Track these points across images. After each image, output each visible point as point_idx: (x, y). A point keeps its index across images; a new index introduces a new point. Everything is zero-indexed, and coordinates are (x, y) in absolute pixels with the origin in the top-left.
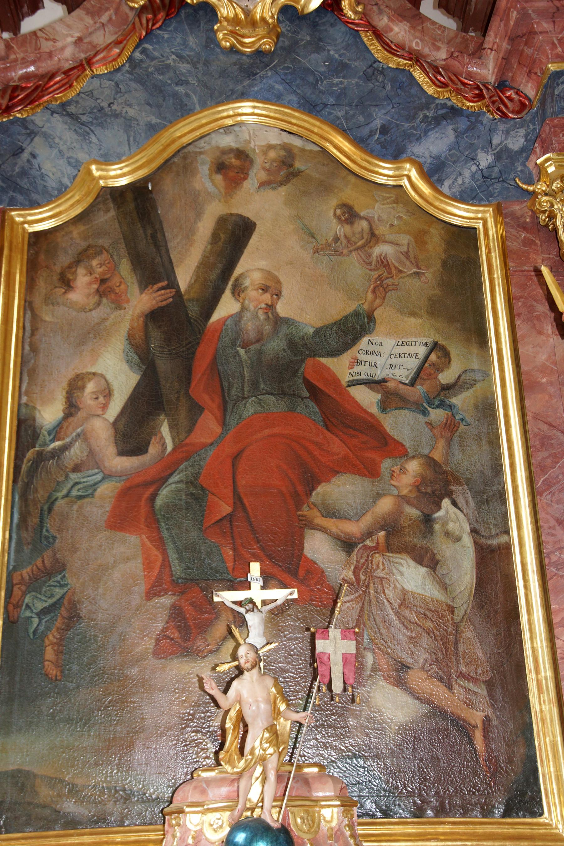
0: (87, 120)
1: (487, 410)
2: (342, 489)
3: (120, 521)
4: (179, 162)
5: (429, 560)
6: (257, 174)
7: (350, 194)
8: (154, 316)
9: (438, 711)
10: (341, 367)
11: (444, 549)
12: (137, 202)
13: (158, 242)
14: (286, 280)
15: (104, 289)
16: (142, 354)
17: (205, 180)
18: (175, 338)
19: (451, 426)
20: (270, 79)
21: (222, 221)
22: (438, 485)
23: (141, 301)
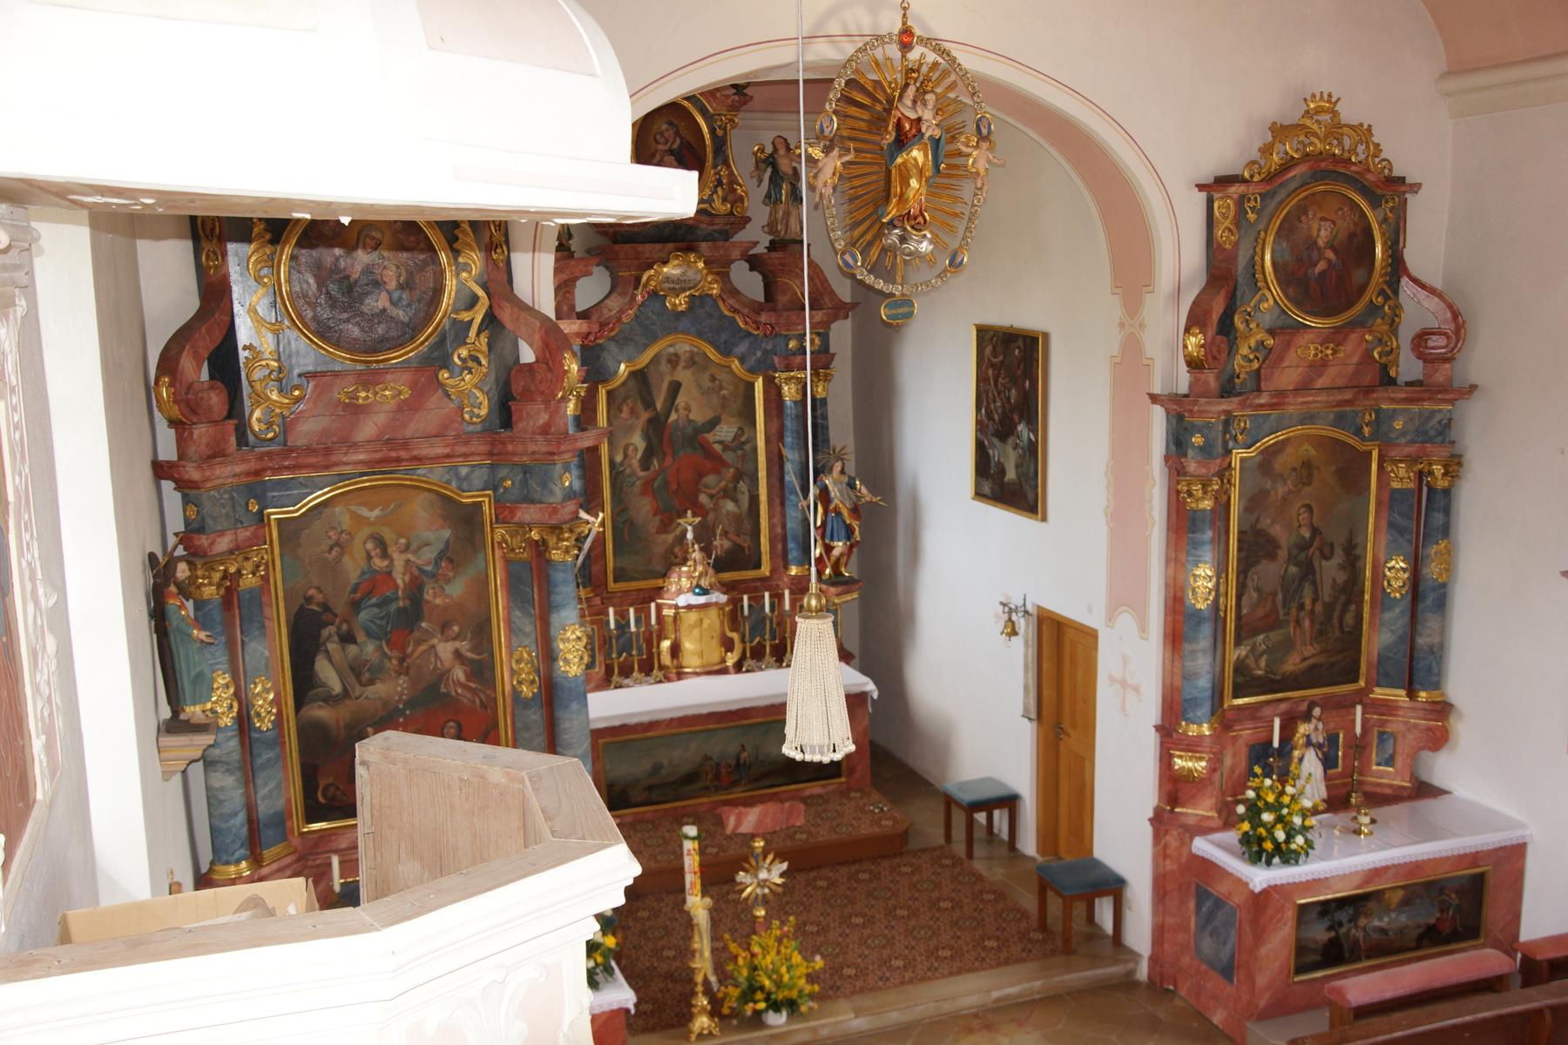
0: (623, 341)
1: (755, 449)
2: (710, 479)
3: (644, 492)
4: (655, 360)
5: (735, 500)
6: (682, 364)
7: (713, 370)
8: (650, 421)
9: (735, 544)
10: (710, 437)
11: (740, 496)
12: (640, 376)
13: (650, 393)
14: (692, 406)
15: (633, 412)
16: (647, 436)
17: (664, 367)
18: (656, 428)
19: (744, 456)
20: (684, 323)
21: (671, 383)
22: (739, 476)
23: (645, 416)
